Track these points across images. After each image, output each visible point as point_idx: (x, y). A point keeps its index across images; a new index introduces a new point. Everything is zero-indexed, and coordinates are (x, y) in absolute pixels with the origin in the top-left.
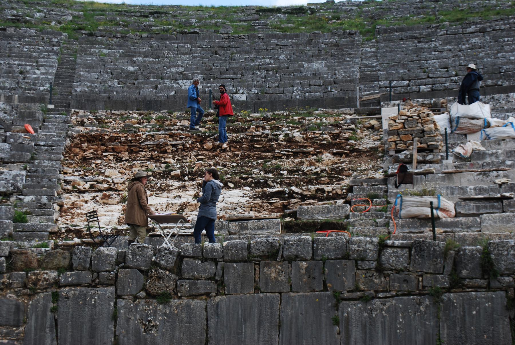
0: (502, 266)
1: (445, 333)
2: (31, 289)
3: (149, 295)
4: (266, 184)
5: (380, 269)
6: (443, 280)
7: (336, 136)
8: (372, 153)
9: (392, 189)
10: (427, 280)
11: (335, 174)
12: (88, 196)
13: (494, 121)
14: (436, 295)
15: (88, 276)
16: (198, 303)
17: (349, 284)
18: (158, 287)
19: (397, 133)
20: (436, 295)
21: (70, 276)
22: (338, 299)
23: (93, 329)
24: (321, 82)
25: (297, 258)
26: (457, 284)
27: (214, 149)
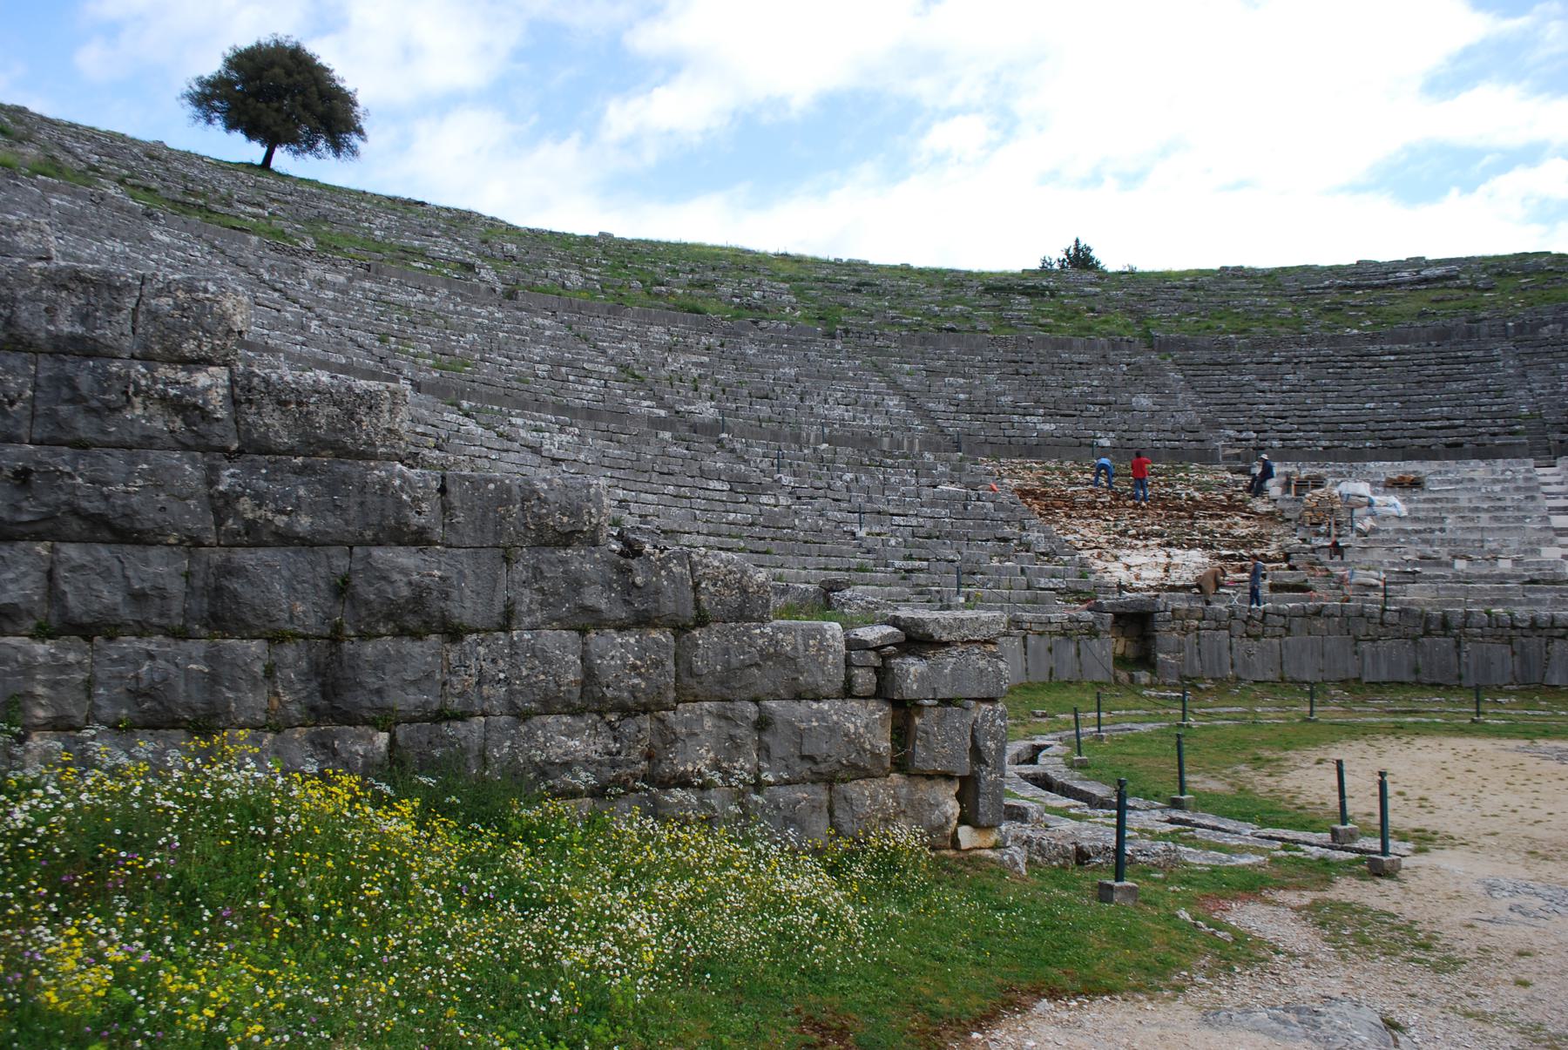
0: (1454, 624)
1: (1420, 660)
2: (1185, 630)
3: (1249, 636)
4: (1212, 547)
5: (1382, 624)
6: (1420, 631)
7: (1229, 498)
8: (1270, 516)
9: (1325, 558)
10: (1410, 631)
11: (1261, 539)
12: (1086, 554)
13: (1375, 498)
14: (1415, 639)
15: (1214, 624)
16: (1276, 641)
17: (1363, 631)
18: (1253, 631)
19: (1312, 510)
20: (1415, 639)
21: (1204, 624)
22: (1357, 640)
23: (1220, 655)
24: (1169, 427)
25: (1332, 615)
26: (1427, 633)
27: (1135, 507)
